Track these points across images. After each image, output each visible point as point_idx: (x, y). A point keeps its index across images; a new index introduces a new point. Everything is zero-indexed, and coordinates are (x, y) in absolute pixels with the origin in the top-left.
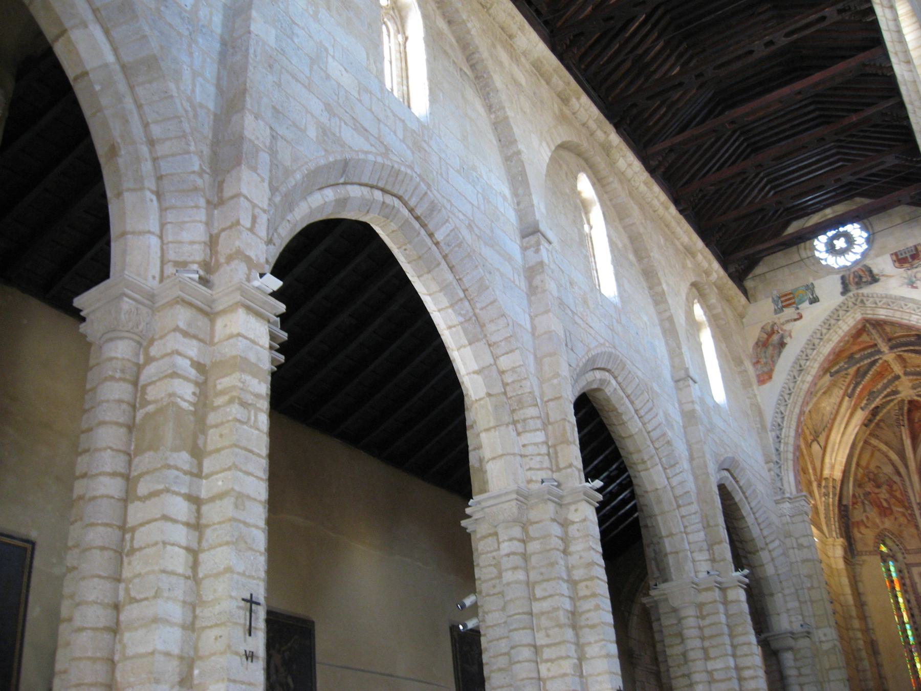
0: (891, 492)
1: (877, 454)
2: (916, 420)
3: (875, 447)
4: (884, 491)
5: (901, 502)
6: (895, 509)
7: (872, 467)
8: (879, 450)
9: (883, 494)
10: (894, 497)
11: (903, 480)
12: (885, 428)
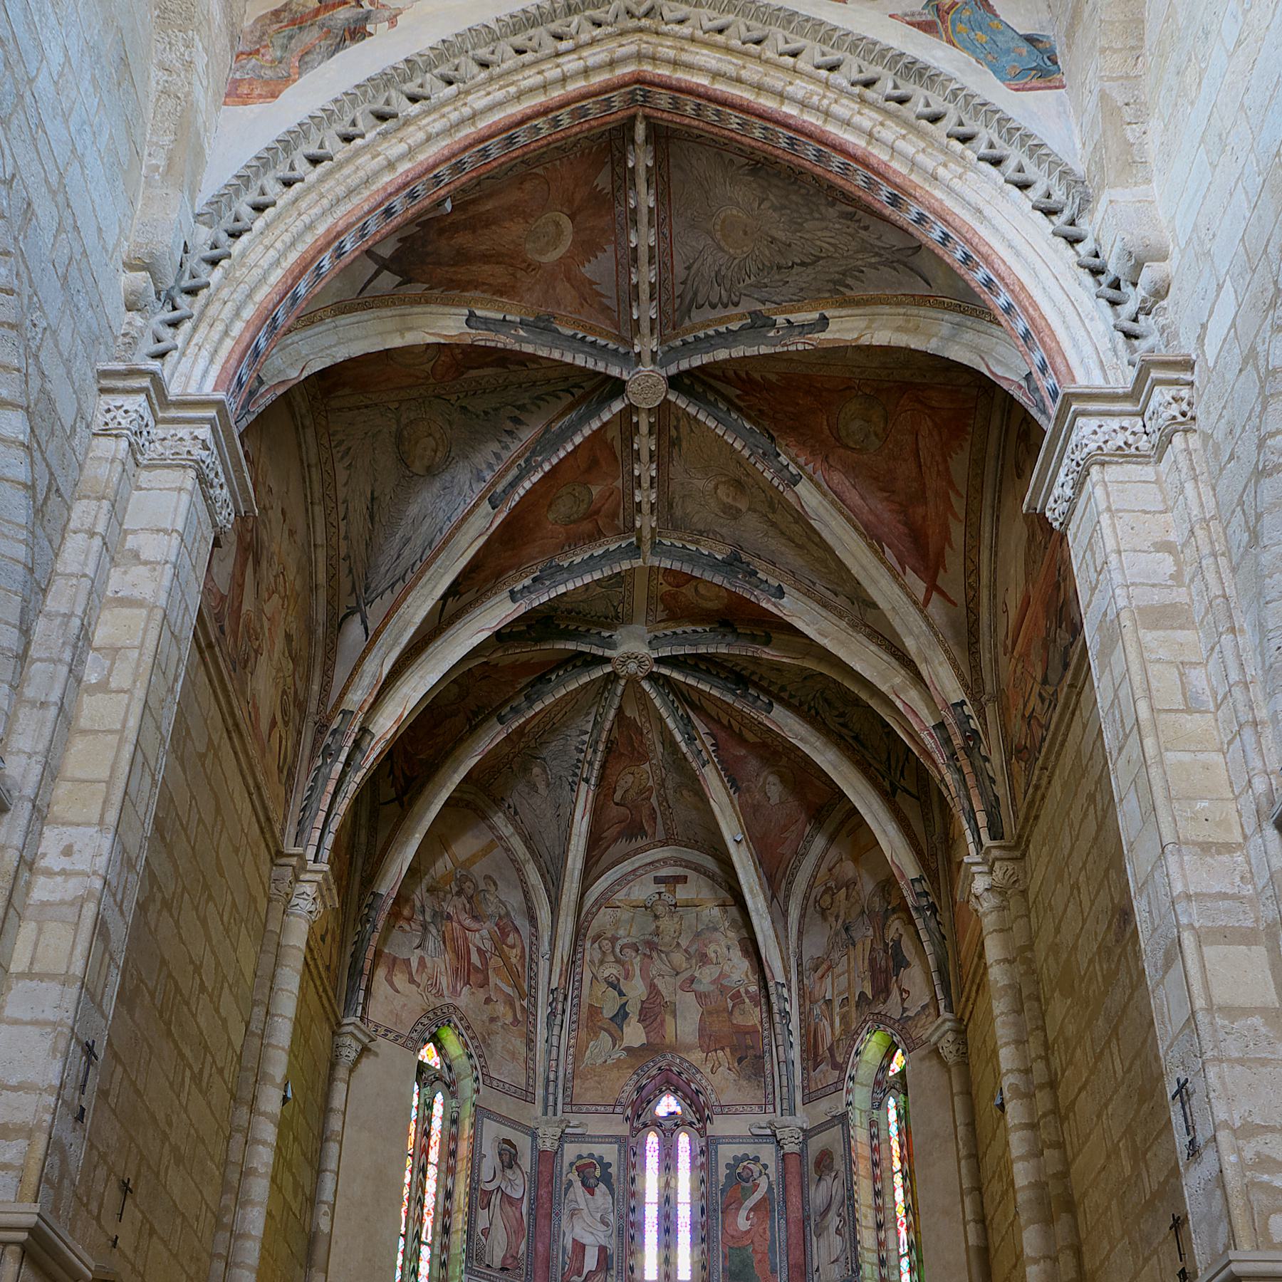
0: (500, 940)
1: (498, 852)
2: (618, 797)
3: (500, 838)
4: (484, 932)
5: (515, 977)
6: (493, 979)
7: (478, 870)
8: (507, 850)
9: (481, 937)
10: (502, 955)
11: (536, 935)
12: (541, 787)
